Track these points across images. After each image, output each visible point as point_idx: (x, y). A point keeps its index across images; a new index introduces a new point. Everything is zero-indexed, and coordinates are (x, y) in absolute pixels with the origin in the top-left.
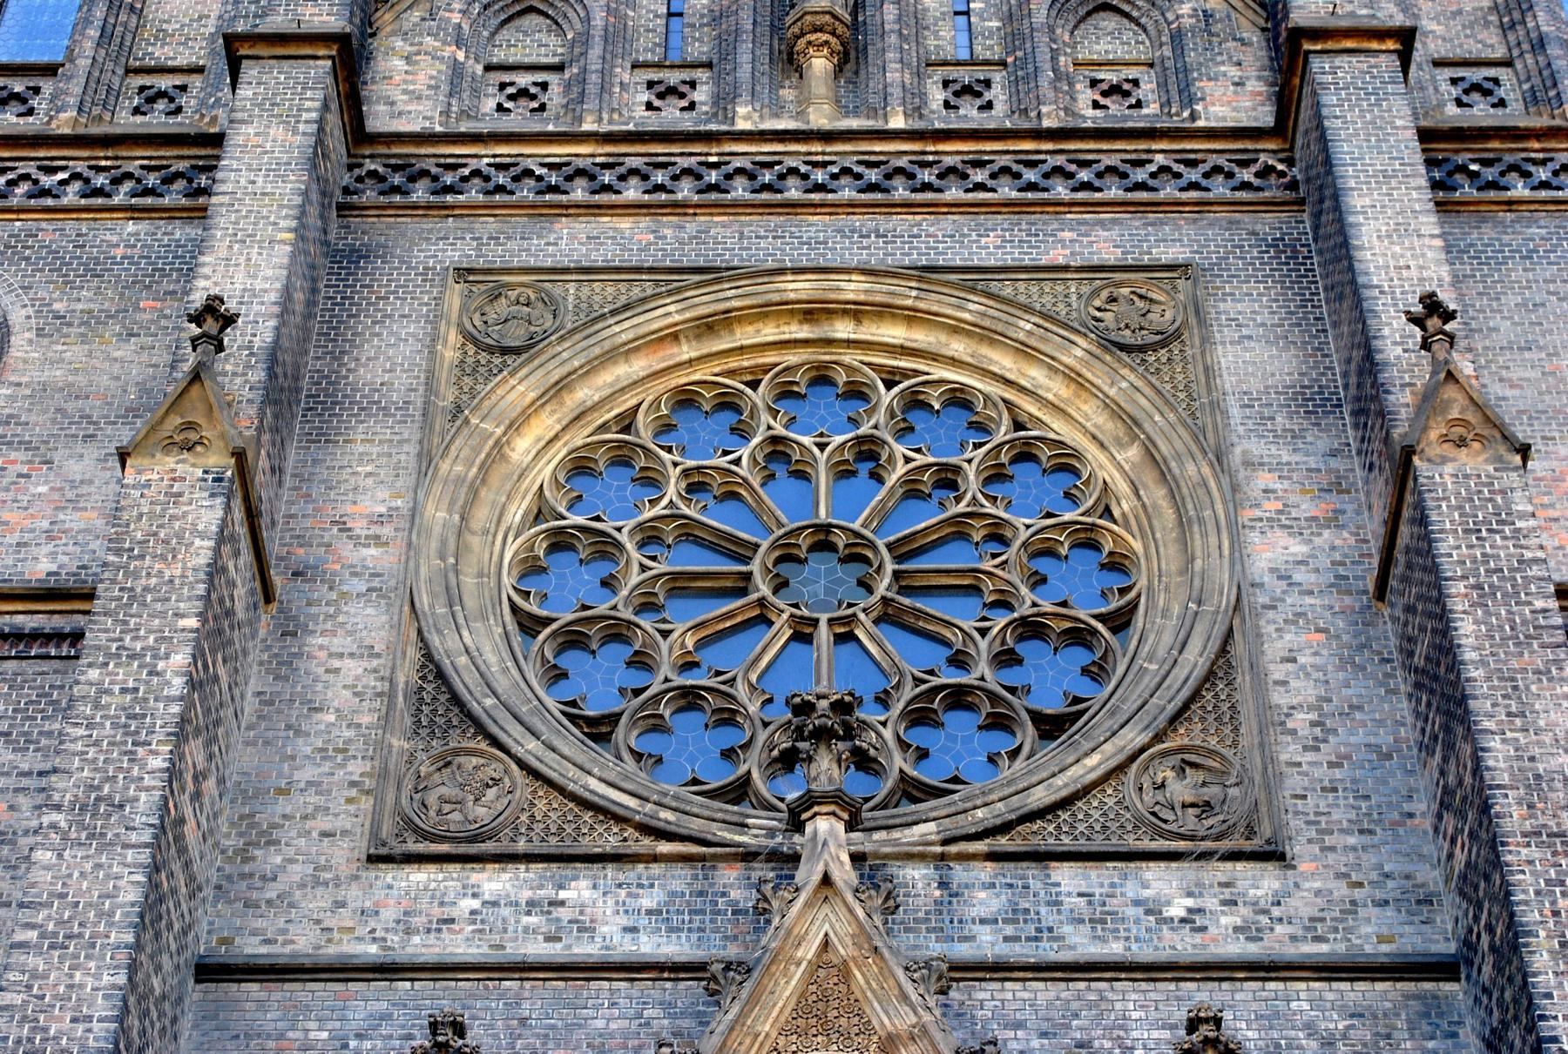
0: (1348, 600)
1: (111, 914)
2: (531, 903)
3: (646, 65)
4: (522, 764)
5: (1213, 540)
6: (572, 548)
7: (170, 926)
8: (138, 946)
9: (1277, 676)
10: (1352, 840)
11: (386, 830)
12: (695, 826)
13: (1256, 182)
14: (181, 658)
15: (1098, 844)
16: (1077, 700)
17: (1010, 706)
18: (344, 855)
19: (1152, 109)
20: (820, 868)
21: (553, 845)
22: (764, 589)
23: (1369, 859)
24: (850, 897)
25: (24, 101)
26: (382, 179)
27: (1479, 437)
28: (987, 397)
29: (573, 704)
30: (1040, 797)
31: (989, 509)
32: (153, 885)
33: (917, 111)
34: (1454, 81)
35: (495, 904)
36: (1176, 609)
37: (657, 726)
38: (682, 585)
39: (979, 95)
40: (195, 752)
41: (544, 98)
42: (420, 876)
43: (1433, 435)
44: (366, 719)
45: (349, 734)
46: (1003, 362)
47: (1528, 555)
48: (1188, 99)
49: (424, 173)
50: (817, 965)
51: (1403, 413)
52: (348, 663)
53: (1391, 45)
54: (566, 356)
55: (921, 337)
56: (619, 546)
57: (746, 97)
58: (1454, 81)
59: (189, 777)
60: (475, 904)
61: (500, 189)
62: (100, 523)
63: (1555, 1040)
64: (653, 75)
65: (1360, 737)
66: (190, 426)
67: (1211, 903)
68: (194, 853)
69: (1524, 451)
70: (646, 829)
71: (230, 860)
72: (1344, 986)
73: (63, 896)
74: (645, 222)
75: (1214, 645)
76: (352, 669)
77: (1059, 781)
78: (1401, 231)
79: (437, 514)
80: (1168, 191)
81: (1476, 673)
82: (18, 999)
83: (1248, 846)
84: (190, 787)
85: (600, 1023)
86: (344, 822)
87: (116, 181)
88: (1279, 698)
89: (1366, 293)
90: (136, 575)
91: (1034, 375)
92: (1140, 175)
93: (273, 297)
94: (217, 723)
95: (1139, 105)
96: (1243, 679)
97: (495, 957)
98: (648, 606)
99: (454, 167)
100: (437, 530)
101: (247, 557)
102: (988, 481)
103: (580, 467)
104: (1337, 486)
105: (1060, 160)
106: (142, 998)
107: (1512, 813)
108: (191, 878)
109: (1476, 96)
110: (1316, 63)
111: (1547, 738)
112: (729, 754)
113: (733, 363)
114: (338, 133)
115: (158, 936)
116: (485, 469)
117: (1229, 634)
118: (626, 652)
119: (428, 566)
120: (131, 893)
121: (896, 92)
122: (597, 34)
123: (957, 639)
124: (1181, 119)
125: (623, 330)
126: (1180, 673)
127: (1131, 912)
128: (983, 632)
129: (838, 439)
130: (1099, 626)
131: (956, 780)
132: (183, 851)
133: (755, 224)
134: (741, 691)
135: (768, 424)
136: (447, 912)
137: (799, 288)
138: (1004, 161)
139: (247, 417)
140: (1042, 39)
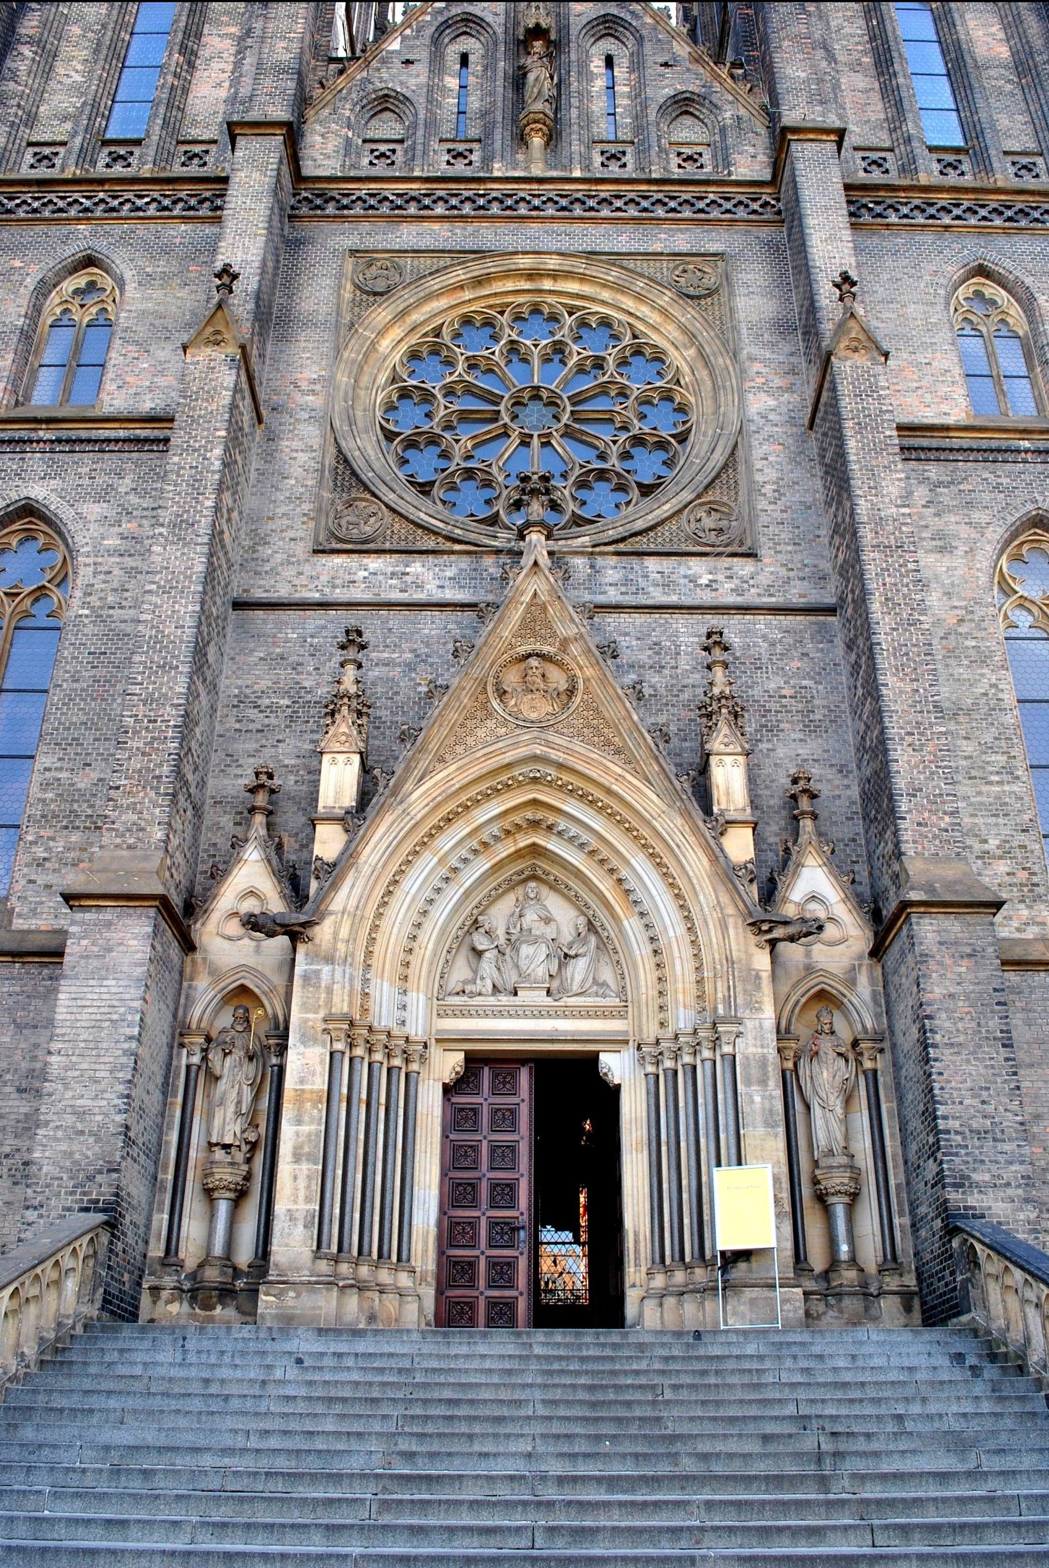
0: (795, 429)
1: (191, 577)
2: (393, 574)
3: (447, 140)
4: (387, 506)
5: (730, 397)
6: (411, 397)
7: (219, 583)
8: (205, 593)
9: (758, 467)
10: (790, 548)
11: (322, 537)
12: (472, 537)
13: (760, 210)
14: (218, 451)
15: (667, 548)
16: (660, 477)
17: (627, 479)
18: (302, 549)
19: (708, 169)
20: (533, 558)
21: (403, 545)
22: (506, 419)
23: (798, 557)
24: (547, 572)
25: (125, 159)
26: (311, 201)
27: (864, 347)
28: (619, 321)
29: (412, 476)
30: (640, 525)
31: (619, 379)
32: (210, 563)
33: (587, 168)
34: (864, 159)
35: (375, 574)
36: (710, 432)
37: (453, 488)
38: (465, 417)
39: (619, 159)
40: (227, 498)
41: (394, 158)
42: (338, 560)
43: (842, 345)
44: (310, 483)
45: (302, 490)
46: (629, 303)
47: (884, 408)
48: (728, 164)
49: (333, 198)
50: (530, 605)
51: (828, 334)
52: (300, 454)
53: (833, 137)
54: (406, 297)
55: (587, 289)
56: (434, 396)
57: (498, 158)
58: (864, 159)
59: (225, 511)
60: (366, 574)
61: (372, 207)
62: (175, 383)
63: (879, 644)
64: (451, 146)
65: (797, 498)
66: (218, 332)
67: (720, 577)
68: (229, 548)
69: (886, 355)
70: (448, 538)
71: (246, 551)
72: (782, 618)
73: (167, 568)
74: (446, 226)
75: (728, 451)
76: (303, 457)
77: (649, 517)
78: (832, 238)
80: (715, 214)
82: (149, 617)
83: (740, 550)
84: (226, 515)
85: (426, 631)
86: (300, 534)
87: (175, 203)
88: (759, 478)
89: (813, 270)
90: (194, 409)
91: (644, 310)
92: (701, 205)
93: (257, 264)
94: (237, 484)
95: (702, 167)
96: (741, 468)
97: (376, 599)
98: (448, 427)
99: (348, 195)
100: (343, 387)
101: (248, 400)
102: (619, 365)
103: (414, 355)
104: (793, 371)
105: (660, 196)
106: (207, 618)
107: (867, 535)
108: (228, 560)
109: (874, 167)
110: (794, 146)
111: (887, 500)
112: (488, 502)
113: (492, 301)
114: (287, 176)
115: (213, 588)
116: (366, 356)
117: (736, 445)
118: (438, 450)
119: (339, 405)
120: (200, 568)
121: (576, 157)
122: (421, 122)
123: (601, 446)
124: (723, 175)
125: (435, 283)
126: (710, 465)
127: (682, 581)
128: (615, 442)
129: (544, 342)
130: (672, 440)
131: (599, 516)
132: (223, 547)
133: (502, 227)
134: (494, 470)
135: (509, 334)
136: (352, 577)
137: (525, 262)
138: (632, 195)
139: (246, 329)
140: (653, 129)
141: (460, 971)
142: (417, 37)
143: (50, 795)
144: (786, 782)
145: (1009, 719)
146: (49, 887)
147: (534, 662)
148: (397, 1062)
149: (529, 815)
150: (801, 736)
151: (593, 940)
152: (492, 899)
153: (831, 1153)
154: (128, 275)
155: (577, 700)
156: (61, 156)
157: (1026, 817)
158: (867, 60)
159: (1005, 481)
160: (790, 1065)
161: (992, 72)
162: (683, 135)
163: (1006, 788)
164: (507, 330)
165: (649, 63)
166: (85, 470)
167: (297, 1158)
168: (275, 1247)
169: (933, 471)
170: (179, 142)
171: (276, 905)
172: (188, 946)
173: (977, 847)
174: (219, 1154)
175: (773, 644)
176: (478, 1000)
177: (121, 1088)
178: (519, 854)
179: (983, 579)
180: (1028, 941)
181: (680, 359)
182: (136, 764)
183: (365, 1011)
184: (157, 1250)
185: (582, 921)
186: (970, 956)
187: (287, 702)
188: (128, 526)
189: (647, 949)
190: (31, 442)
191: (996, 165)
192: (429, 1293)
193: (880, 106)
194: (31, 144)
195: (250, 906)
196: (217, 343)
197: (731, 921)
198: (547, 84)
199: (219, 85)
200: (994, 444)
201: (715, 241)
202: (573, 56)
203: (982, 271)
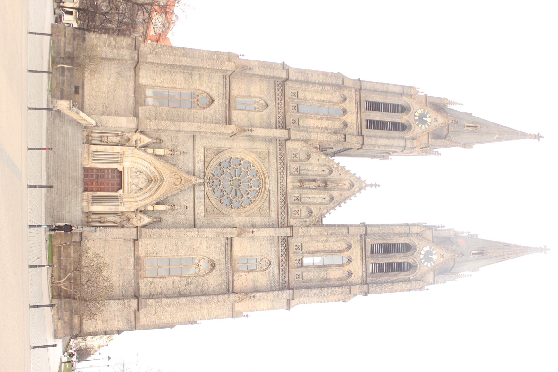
11: (207, 148)
12: (208, 171)
14: (214, 131)
18: (205, 145)
19: (294, 216)
30: (210, 199)
46: (259, 199)
52: (224, 144)
54: (259, 161)
55: (263, 192)
64: (298, 168)
67: (201, 211)
74: (276, 167)
76: (223, 144)
79: (240, 150)
81: (214, 229)
92: (283, 213)
105: (285, 205)
120: (193, 130)
122: (302, 162)
125: (262, 165)
133: (276, 178)
134: (223, 176)
137: (267, 181)
138: (284, 201)
141: (134, 170)
142: (325, 161)
143: (161, 110)
144: (164, 218)
145: (176, 254)
146: (146, 111)
147: (180, 180)
148: (119, 161)
149: (157, 179)
150: (172, 221)
151: (139, 189)
152: (145, 175)
153: (107, 219)
154: (263, 112)
155: (174, 186)
156: (295, 97)
157: (159, 254)
158: (327, 249)
159: (222, 260)
160: (119, 214)
161: (325, 274)
162: (303, 212)
163: (164, 252)
164: (254, 178)
165: (320, 206)
166: (220, 109)
167: (105, 148)
168: (93, 146)
169: (223, 248)
170: (298, 119)
171: (140, 145)
172: (135, 132)
173: (154, 246)
174: (106, 138)
175: (188, 218)
176: (130, 173)
177: (112, 126)
178: (151, 178)
179: (202, 254)
180: (138, 251)
181: (248, 208)
182: (160, 124)
183: (126, 156)
184: (93, 131)
185: (142, 188)
186: (131, 235)
187: (177, 144)
188: (209, 117)
189: (136, 196)
190: (226, 100)
191: (296, 269)
192: (88, 166)
193: (313, 250)
194: (297, 91)
195: (142, 140)
196: (237, 130)
197: (138, 206)
198: (312, 186)
199: (314, 124)
200: (229, 259)
201: (274, 215)
202: (321, 191)
203: (270, 263)
